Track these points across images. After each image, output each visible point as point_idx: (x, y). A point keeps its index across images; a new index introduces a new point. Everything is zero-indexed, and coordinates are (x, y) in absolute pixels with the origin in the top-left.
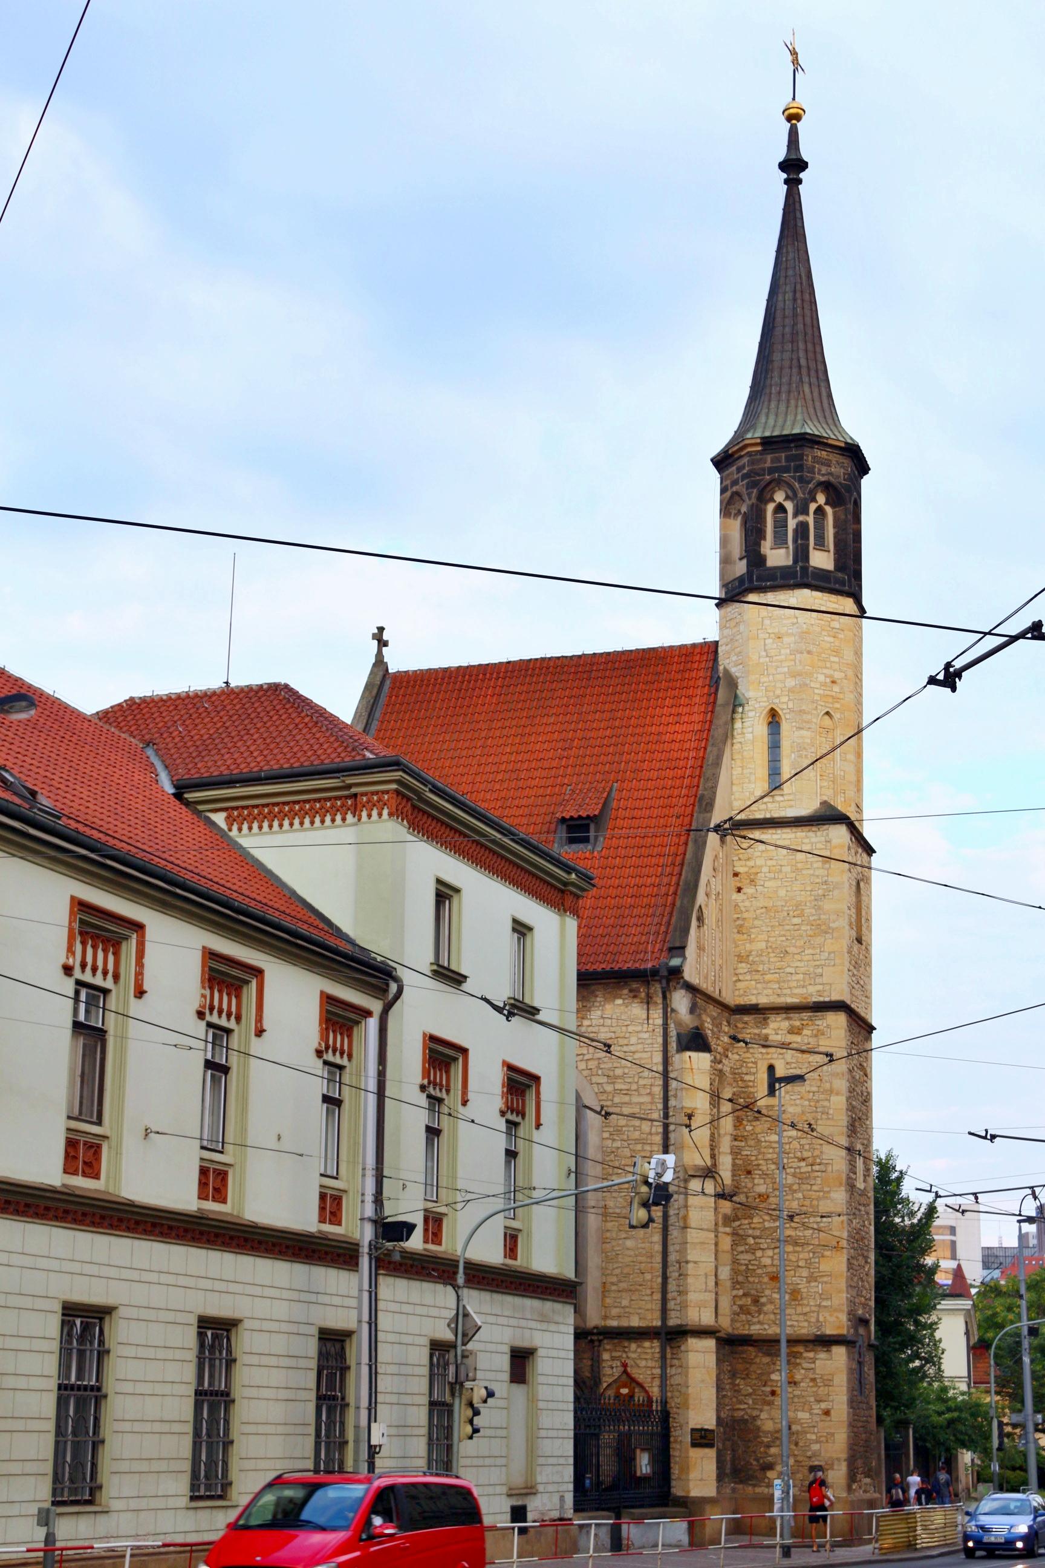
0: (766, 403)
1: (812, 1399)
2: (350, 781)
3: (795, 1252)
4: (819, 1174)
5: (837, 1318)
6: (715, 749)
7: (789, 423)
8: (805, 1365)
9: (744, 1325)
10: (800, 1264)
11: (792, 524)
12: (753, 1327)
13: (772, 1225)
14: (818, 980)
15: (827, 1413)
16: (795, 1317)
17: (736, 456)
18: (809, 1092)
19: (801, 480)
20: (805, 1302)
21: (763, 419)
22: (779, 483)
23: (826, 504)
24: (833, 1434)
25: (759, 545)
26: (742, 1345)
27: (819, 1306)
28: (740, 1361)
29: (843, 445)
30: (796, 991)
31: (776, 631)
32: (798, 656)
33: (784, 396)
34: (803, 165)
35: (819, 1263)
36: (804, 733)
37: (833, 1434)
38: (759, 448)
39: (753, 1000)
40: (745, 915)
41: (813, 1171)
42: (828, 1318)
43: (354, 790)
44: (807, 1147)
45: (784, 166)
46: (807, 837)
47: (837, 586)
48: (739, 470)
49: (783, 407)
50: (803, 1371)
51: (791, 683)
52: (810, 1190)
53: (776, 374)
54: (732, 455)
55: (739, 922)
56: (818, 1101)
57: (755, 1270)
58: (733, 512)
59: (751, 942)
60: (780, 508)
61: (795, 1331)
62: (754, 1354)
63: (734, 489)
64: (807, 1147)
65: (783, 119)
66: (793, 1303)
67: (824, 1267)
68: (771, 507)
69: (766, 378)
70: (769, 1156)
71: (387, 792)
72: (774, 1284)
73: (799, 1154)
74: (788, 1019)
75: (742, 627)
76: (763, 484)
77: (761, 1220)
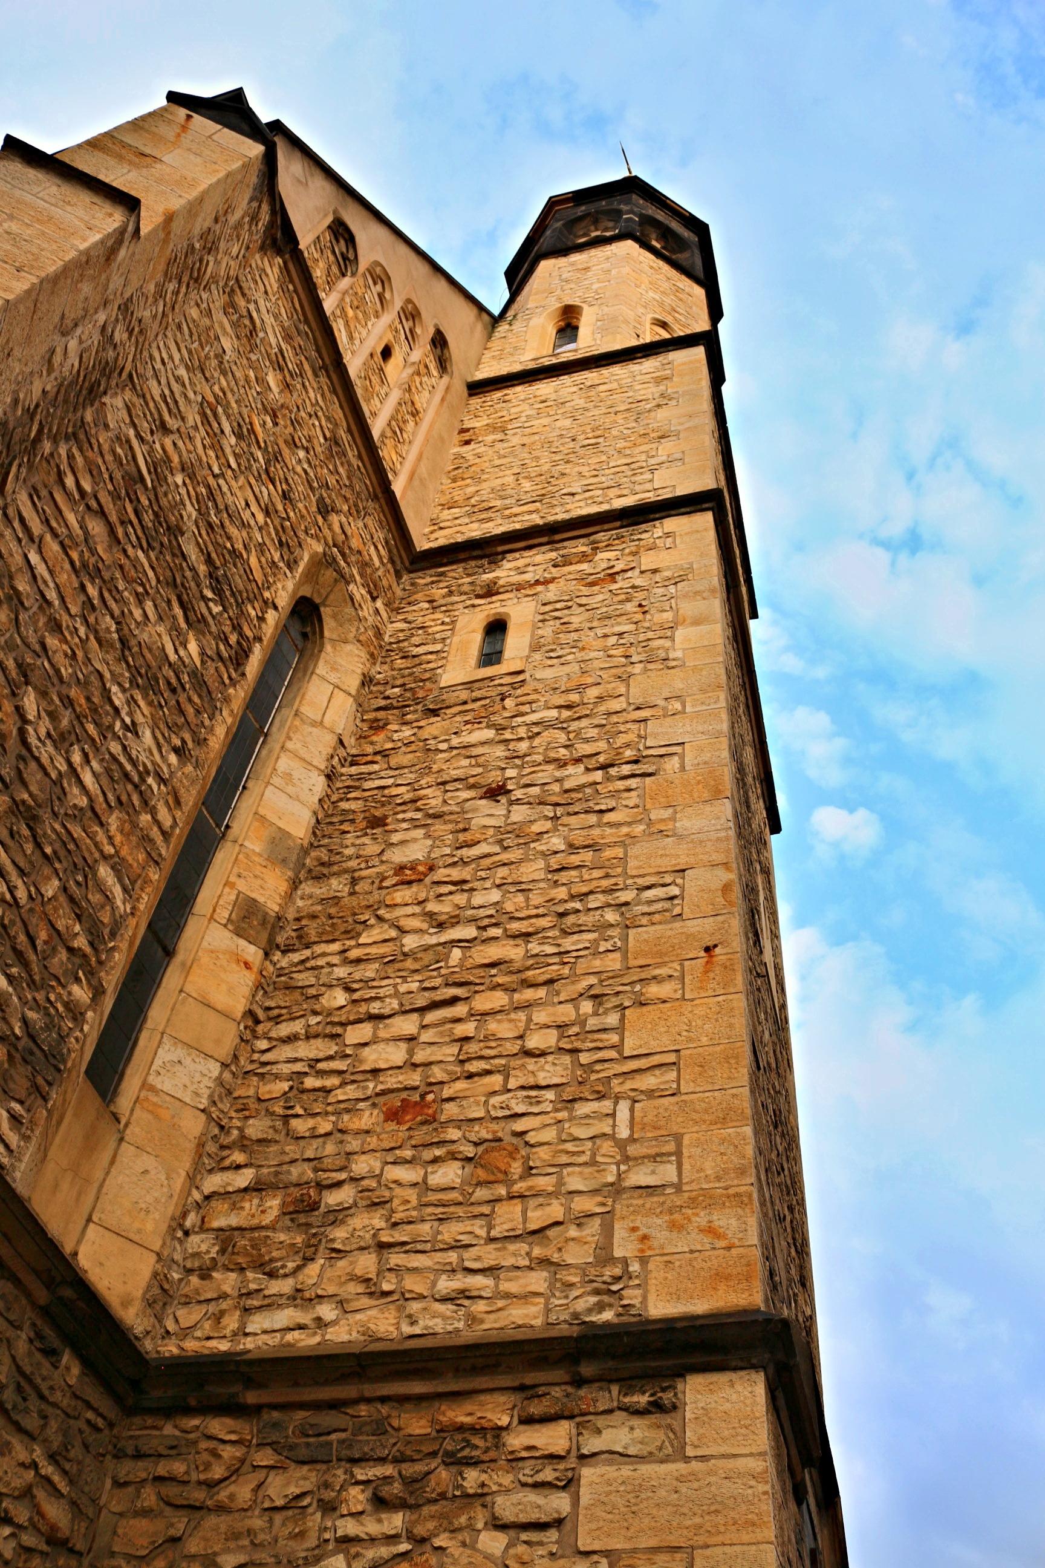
4: (633, 783)
5: (710, 1230)
9: (218, 1317)
12: (255, 1325)
13: (433, 940)
18: (606, 636)
20: (544, 1183)
27: (616, 1189)
28: (149, 1497)
35: (620, 1029)
42: (661, 1236)
50: (493, 1543)
57: (328, 1091)
61: (473, 1319)
62: (228, 1452)
64: (593, 733)
66: (481, 1194)
77: (393, 933)
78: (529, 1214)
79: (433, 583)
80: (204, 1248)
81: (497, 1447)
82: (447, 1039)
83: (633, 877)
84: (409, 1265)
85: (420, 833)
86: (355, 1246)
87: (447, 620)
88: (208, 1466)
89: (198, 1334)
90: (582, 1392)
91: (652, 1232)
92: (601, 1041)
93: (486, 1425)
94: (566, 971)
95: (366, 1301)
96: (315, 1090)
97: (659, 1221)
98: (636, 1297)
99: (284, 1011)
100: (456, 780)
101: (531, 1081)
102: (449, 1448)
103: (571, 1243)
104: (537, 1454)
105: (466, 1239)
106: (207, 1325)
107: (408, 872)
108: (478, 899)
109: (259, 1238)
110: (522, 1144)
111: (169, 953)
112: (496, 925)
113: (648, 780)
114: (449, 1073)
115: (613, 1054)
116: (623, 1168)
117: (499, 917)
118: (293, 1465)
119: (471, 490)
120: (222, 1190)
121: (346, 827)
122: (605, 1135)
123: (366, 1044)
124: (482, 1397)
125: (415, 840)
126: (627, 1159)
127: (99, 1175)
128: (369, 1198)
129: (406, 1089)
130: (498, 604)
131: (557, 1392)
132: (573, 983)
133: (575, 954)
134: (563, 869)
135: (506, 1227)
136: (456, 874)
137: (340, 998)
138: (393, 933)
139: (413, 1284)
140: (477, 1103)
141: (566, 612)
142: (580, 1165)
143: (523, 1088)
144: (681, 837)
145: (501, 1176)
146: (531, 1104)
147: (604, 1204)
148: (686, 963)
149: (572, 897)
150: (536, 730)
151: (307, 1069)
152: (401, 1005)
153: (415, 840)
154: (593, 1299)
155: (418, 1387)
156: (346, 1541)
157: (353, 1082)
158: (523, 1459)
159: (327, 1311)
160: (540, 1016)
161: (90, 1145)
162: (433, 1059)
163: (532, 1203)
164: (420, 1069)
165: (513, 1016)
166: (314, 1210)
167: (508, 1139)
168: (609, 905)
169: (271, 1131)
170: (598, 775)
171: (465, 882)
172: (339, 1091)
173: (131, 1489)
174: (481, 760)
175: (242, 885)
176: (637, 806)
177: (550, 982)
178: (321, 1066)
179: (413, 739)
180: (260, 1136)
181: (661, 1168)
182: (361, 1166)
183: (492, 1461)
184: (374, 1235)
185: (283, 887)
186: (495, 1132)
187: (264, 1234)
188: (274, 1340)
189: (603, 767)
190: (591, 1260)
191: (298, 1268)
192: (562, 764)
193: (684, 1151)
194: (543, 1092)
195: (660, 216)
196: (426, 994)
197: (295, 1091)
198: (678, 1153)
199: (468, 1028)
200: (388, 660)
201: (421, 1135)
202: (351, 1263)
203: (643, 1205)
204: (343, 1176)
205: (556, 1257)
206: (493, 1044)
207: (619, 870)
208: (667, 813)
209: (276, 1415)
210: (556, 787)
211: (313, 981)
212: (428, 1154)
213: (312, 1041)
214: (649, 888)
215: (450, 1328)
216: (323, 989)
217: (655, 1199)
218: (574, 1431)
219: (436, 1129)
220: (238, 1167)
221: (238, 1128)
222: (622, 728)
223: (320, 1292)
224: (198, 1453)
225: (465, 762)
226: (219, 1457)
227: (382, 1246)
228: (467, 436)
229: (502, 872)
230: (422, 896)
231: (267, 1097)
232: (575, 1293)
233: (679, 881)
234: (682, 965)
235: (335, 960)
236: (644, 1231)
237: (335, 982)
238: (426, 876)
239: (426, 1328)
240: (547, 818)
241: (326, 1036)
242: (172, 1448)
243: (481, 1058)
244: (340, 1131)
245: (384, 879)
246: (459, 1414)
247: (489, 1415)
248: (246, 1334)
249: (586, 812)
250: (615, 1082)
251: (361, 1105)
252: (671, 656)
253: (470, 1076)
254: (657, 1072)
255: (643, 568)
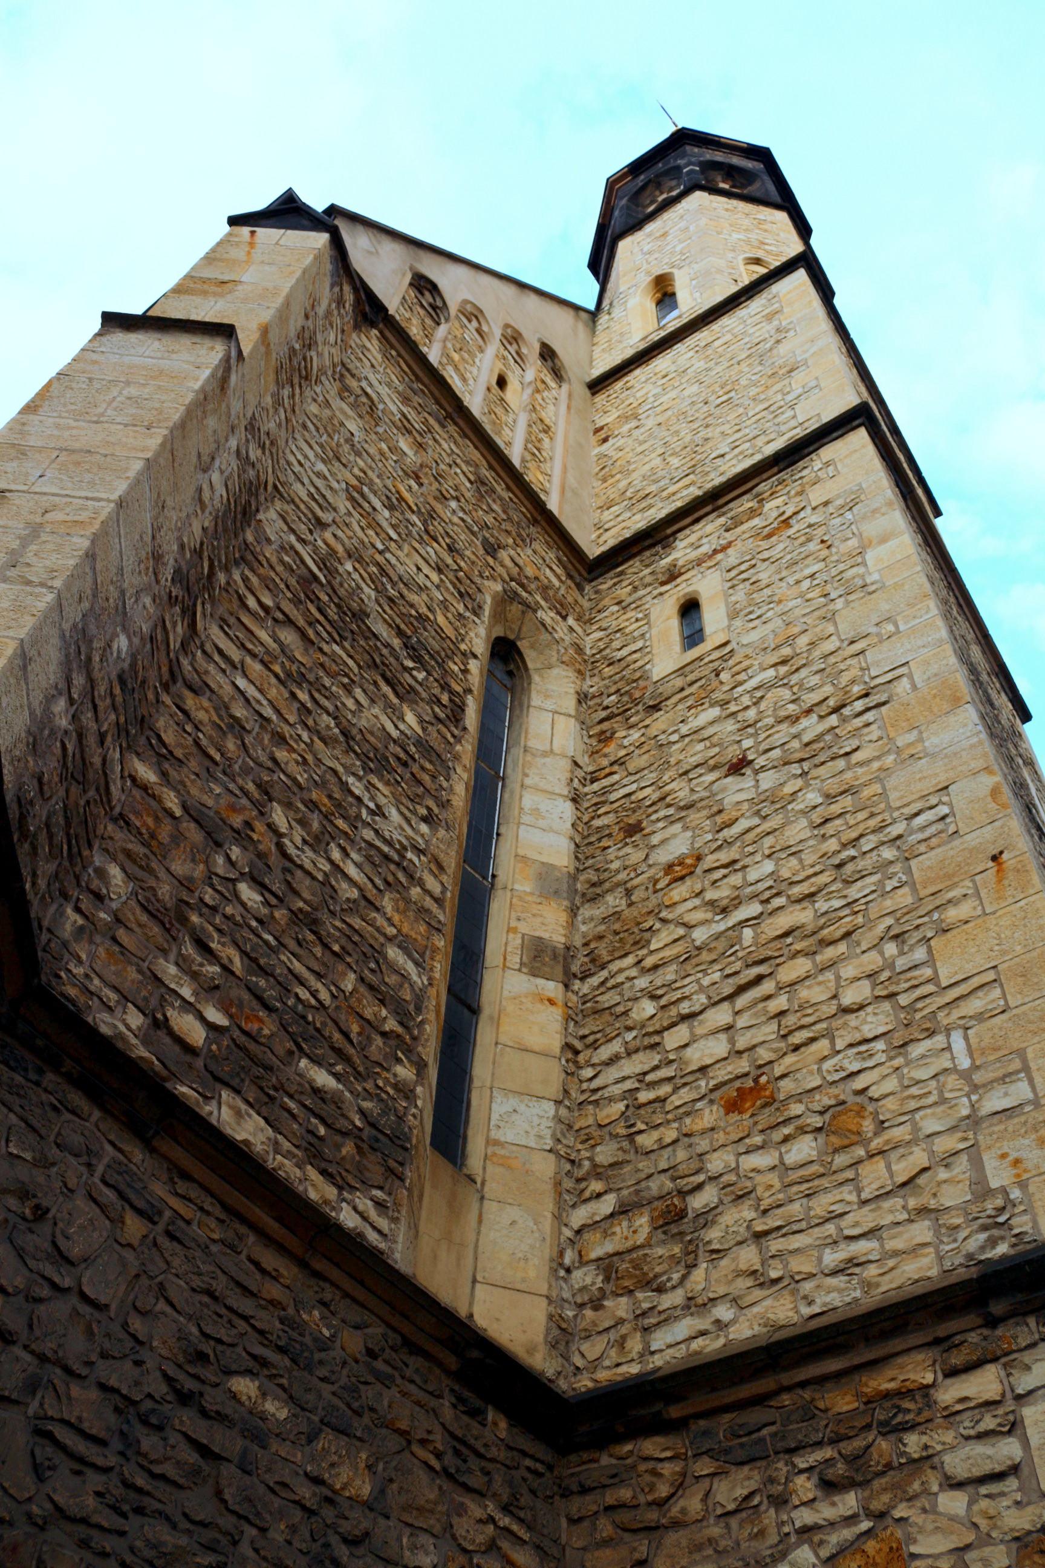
4: (869, 716)
9: (621, 1343)
10: (849, 998)
12: (660, 1339)
13: (722, 927)
18: (798, 582)
20: (899, 1133)
26: (604, 1440)
27: (974, 1121)
28: (605, 1527)
35: (931, 961)
52: (849, 767)
57: (663, 1100)
61: (868, 1286)
62: (668, 1469)
64: (815, 680)
66: (841, 1160)
77: (681, 931)
78: (894, 1168)
79: (615, 584)
80: (588, 1280)
81: (929, 1406)
82: (764, 1019)
83: (898, 808)
84: (791, 1248)
85: (677, 827)
86: (733, 1242)
87: (640, 615)
88: (652, 1488)
89: (607, 1363)
90: (999, 1332)
91: (1023, 1154)
92: (915, 978)
93: (912, 1387)
94: (860, 920)
95: (758, 1293)
96: (650, 1102)
97: (1027, 1142)
98: (1026, 1223)
99: (599, 1036)
100: (696, 767)
101: (858, 1037)
102: (882, 1418)
103: (944, 1186)
104: (972, 1404)
105: (839, 1208)
106: (613, 1353)
107: (677, 868)
108: (753, 875)
109: (638, 1258)
110: (866, 1101)
111: (475, 1011)
112: (778, 894)
113: (883, 709)
114: (775, 1051)
115: (930, 988)
116: (974, 1098)
117: (778, 886)
118: (733, 1468)
119: (623, 484)
120: (590, 1222)
121: (605, 843)
122: (946, 1070)
123: (686, 1046)
124: (899, 1360)
125: (674, 836)
126: (975, 1088)
127: (471, 1237)
128: (732, 1192)
129: (738, 1077)
130: (684, 585)
131: (973, 1337)
132: (870, 929)
133: (863, 901)
134: (827, 821)
135: (874, 1186)
136: (724, 857)
137: (648, 1008)
138: (681, 931)
139: (800, 1265)
140: (811, 1073)
141: (752, 571)
142: (930, 1106)
143: (851, 1045)
144: (933, 755)
145: (855, 1138)
146: (864, 1059)
147: (966, 1139)
148: (977, 878)
149: (844, 846)
150: (758, 694)
151: (637, 1085)
152: (709, 998)
153: (674, 836)
154: (983, 1236)
155: (833, 1365)
156: (806, 1531)
157: (685, 1084)
158: (958, 1412)
159: (724, 1312)
160: (848, 971)
161: (455, 1209)
162: (755, 1041)
163: (894, 1156)
164: (745, 1055)
165: (820, 978)
166: (682, 1218)
167: (851, 1099)
168: (883, 843)
169: (620, 1153)
170: (833, 720)
171: (735, 862)
172: (673, 1098)
173: (586, 1524)
174: (715, 739)
175: (523, 928)
176: (880, 738)
177: (848, 934)
178: (649, 1078)
179: (643, 739)
180: (611, 1160)
181: (1012, 1088)
182: (716, 1163)
183: (928, 1421)
184: (748, 1227)
185: (563, 917)
186: (836, 1096)
187: (641, 1253)
188: (680, 1352)
189: (836, 710)
190: (969, 1197)
191: (684, 1278)
192: (794, 719)
193: (1032, 1065)
194: (872, 1045)
195: (719, 157)
196: (730, 981)
197: (631, 1109)
198: (1026, 1068)
199: (781, 1002)
200: (596, 671)
201: (765, 1118)
202: (733, 1260)
203: (1006, 1130)
204: (701, 1178)
205: (933, 1204)
206: (810, 1011)
207: (882, 806)
208: (912, 736)
209: (702, 1423)
210: (796, 744)
211: (618, 999)
212: (777, 1135)
213: (634, 1057)
214: (917, 814)
215: (848, 1299)
216: (630, 1004)
217: (1016, 1120)
218: (1003, 1373)
219: (778, 1109)
220: (599, 1195)
221: (588, 1158)
222: (842, 666)
223: (711, 1295)
224: (639, 1476)
225: (700, 746)
226: (661, 1475)
227: (759, 1236)
228: (602, 435)
229: (768, 841)
230: (698, 887)
231: (607, 1121)
232: (962, 1235)
233: (945, 799)
234: (973, 881)
235: (633, 972)
236: (1014, 1155)
237: (639, 994)
238: (696, 866)
239: (825, 1304)
240: (795, 776)
241: (646, 1048)
242: (614, 1476)
243: (802, 1027)
244: (686, 1135)
245: (656, 882)
246: (883, 1382)
247: (912, 1376)
248: (653, 1353)
249: (833, 759)
250: (941, 1015)
251: (699, 1105)
252: (868, 581)
253: (796, 1048)
254: (980, 994)
255: (814, 504)
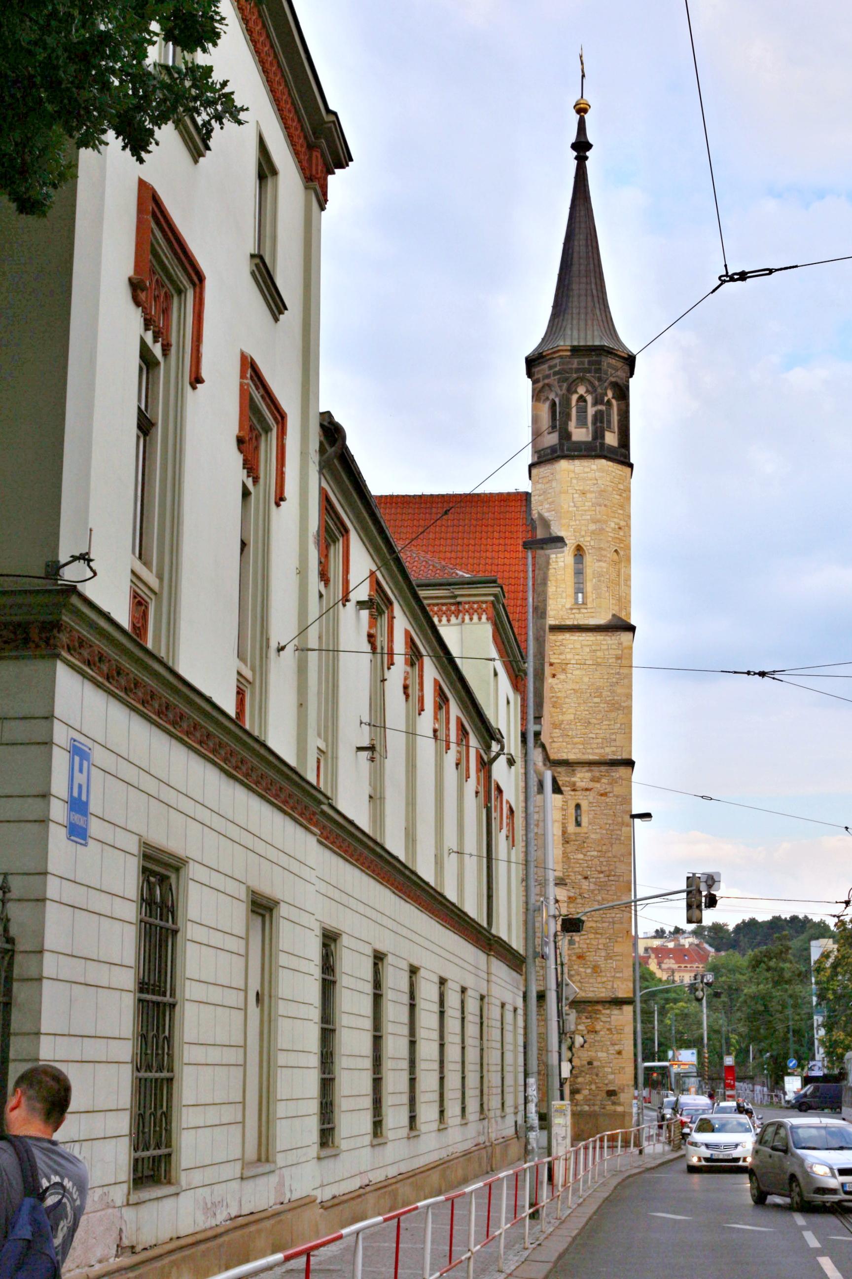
0: (569, 321)
1: (609, 1043)
2: (457, 592)
3: (596, 938)
6: (541, 572)
7: (589, 337)
8: (603, 1019)
10: (600, 947)
11: (591, 411)
14: (612, 744)
15: (619, 1053)
16: (597, 985)
17: (548, 357)
19: (600, 379)
21: (569, 332)
22: (582, 380)
23: (613, 398)
24: (623, 1068)
25: (567, 424)
27: (614, 977)
29: (626, 356)
30: (597, 751)
31: (581, 488)
32: (598, 508)
33: (583, 316)
34: (589, 146)
36: (604, 564)
37: (623, 1068)
38: (569, 353)
39: (564, 756)
40: (559, 694)
41: (609, 880)
43: (459, 599)
44: (605, 863)
45: (574, 146)
46: (604, 640)
47: (622, 459)
48: (550, 368)
49: (582, 324)
51: (592, 527)
53: (575, 299)
54: (545, 356)
55: (554, 699)
56: (613, 830)
58: (543, 398)
59: (563, 714)
60: (581, 399)
63: (546, 381)
64: (605, 863)
65: (574, 111)
67: (618, 949)
68: (575, 397)
69: (567, 302)
70: (577, 869)
71: (486, 602)
72: (579, 961)
73: (599, 869)
74: (591, 771)
75: (554, 484)
76: (571, 380)
199: (588, 941)
